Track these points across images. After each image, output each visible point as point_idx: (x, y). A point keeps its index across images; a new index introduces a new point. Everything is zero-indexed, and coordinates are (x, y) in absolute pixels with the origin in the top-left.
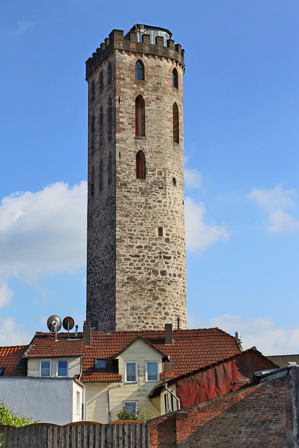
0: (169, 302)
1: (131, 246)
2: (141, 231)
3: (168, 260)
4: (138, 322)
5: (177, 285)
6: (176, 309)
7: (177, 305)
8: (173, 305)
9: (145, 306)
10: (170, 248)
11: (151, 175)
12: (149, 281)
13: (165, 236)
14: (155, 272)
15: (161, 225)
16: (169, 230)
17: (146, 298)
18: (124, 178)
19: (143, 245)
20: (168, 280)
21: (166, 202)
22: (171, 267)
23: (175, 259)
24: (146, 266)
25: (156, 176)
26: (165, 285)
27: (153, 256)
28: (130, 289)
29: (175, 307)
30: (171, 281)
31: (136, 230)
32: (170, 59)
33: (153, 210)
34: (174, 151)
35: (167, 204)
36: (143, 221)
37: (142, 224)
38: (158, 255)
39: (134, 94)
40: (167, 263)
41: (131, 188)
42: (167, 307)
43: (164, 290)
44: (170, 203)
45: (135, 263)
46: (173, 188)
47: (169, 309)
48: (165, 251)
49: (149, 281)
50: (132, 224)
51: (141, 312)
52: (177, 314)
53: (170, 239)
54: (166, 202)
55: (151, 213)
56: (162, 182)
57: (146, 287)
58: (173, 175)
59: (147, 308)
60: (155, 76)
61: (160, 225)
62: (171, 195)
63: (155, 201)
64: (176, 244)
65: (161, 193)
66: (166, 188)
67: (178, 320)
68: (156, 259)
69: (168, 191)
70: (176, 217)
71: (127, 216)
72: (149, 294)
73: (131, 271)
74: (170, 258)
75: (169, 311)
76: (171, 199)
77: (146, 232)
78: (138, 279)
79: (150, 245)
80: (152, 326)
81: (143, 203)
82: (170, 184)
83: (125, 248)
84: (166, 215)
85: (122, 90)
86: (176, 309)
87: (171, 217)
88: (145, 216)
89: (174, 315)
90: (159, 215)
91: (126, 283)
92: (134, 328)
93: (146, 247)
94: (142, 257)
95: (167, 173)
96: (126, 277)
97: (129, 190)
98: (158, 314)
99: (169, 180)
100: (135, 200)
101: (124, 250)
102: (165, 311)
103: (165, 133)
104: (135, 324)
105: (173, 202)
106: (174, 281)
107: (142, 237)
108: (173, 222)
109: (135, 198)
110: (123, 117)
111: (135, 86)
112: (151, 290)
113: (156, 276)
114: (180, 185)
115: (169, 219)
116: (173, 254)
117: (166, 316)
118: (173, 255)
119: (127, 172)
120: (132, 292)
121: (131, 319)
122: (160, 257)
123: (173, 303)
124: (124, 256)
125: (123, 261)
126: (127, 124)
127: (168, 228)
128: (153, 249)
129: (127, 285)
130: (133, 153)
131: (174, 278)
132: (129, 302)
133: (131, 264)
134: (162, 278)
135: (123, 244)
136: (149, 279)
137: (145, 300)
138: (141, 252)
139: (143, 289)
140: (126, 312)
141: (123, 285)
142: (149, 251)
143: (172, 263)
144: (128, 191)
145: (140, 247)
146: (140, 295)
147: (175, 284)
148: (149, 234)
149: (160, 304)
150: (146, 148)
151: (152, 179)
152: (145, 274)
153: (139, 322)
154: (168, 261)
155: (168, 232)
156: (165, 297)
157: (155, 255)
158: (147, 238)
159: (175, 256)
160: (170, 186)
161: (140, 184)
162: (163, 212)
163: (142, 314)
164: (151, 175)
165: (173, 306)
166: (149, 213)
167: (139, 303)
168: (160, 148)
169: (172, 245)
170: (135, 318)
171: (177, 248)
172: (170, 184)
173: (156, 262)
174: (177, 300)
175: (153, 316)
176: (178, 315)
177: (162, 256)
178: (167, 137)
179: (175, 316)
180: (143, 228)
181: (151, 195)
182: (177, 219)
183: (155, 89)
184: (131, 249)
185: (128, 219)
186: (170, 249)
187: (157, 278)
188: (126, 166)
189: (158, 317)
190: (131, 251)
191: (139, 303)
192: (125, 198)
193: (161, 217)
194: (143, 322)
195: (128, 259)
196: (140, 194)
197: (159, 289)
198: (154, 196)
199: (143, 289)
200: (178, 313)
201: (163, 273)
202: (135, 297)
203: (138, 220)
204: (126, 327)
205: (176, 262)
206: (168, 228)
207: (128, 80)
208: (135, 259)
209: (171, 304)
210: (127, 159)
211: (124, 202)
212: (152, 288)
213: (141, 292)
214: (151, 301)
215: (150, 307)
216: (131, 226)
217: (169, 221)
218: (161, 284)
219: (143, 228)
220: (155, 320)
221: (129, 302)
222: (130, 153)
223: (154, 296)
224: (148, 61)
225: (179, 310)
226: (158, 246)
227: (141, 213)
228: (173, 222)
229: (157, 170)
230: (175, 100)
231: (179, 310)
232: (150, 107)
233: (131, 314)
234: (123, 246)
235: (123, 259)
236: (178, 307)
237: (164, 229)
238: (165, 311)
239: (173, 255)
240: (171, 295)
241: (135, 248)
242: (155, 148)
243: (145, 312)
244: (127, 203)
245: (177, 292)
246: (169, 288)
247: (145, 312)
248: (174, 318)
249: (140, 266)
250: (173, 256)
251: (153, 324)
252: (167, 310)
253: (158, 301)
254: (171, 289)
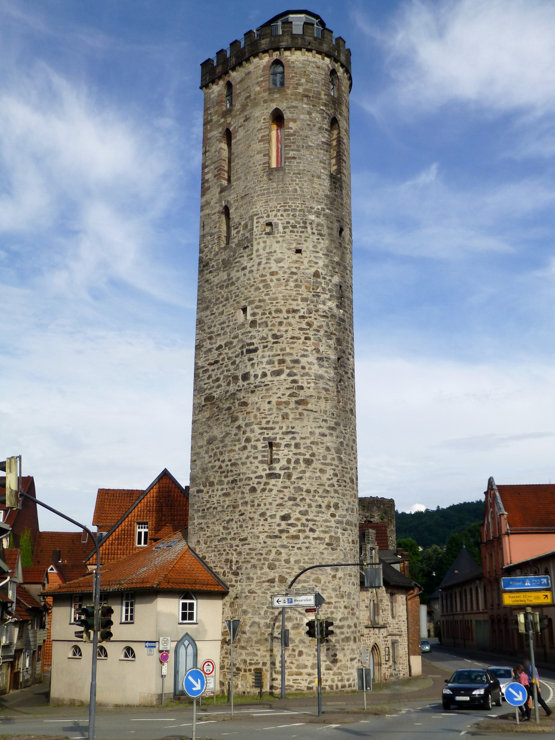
0: (252, 420)
1: (210, 350)
2: (220, 324)
3: (253, 354)
4: (213, 461)
5: (267, 390)
6: (266, 428)
7: (268, 422)
8: (260, 423)
9: (222, 435)
10: (256, 334)
11: (235, 235)
12: (228, 394)
14: (236, 378)
15: (244, 304)
16: (257, 307)
17: (223, 423)
18: (207, 256)
19: (223, 343)
20: (252, 386)
21: (253, 266)
22: (258, 364)
23: (266, 349)
24: (225, 373)
25: (242, 232)
26: (247, 395)
27: (234, 355)
28: (207, 414)
29: (264, 425)
30: (256, 387)
31: (217, 323)
32: (283, 49)
33: (236, 285)
34: (270, 182)
35: (254, 268)
36: (224, 308)
37: (222, 313)
38: (240, 351)
39: (220, 133)
40: (250, 359)
42: (248, 429)
43: (245, 404)
44: (259, 264)
45: (214, 373)
46: (264, 240)
47: (252, 431)
48: (249, 341)
49: (228, 394)
50: (212, 317)
51: (217, 446)
52: (267, 436)
53: (258, 321)
54: (253, 266)
55: (234, 291)
56: (247, 237)
57: (224, 406)
58: (267, 219)
59: (224, 437)
60: (243, 91)
61: (243, 303)
62: (261, 252)
63: (238, 271)
64: (270, 324)
65: (245, 255)
66: (252, 245)
67: (271, 445)
68: (237, 359)
69: (255, 248)
70: (272, 281)
72: (227, 416)
73: (209, 387)
74: (256, 350)
75: (252, 435)
76: (261, 257)
77: (227, 322)
78: (216, 396)
79: (231, 340)
80: (229, 463)
81: (225, 281)
82: (260, 234)
83: (204, 356)
84: (253, 285)
86: (266, 428)
87: (261, 285)
88: (227, 299)
89: (261, 439)
90: (243, 289)
91: (204, 406)
92: (209, 471)
93: (226, 345)
94: (221, 362)
95: (255, 221)
96: (203, 398)
97: (211, 269)
98: (237, 443)
100: (216, 280)
101: (202, 360)
102: (245, 436)
103: (254, 163)
104: (210, 465)
105: (264, 261)
106: (262, 385)
107: (223, 332)
108: (263, 292)
109: (216, 279)
111: (222, 120)
112: (229, 408)
113: (236, 384)
114: (284, 228)
115: (258, 289)
116: (263, 341)
117: (247, 444)
118: (262, 343)
119: (210, 246)
120: (209, 419)
121: (207, 459)
122: (242, 352)
123: (259, 420)
124: (203, 367)
125: (201, 375)
126: (213, 178)
127: (255, 304)
128: (234, 345)
129: (204, 408)
130: (217, 214)
131: (263, 380)
132: (205, 434)
133: (209, 377)
134: (243, 386)
135: (202, 351)
136: (228, 391)
137: (223, 425)
138: (220, 354)
139: (220, 409)
140: (201, 450)
141: (200, 411)
142: (229, 349)
143: (260, 356)
144: (210, 272)
145: (220, 347)
146: (217, 420)
147: (265, 388)
148: (231, 323)
149: (239, 427)
151: (236, 240)
153: (215, 461)
154: (252, 355)
155: (256, 310)
156: (247, 413)
157: (237, 353)
158: (228, 330)
159: (265, 344)
160: (259, 238)
162: (249, 282)
163: (218, 448)
164: (235, 235)
165: (259, 426)
166: (231, 291)
167: (217, 432)
168: (246, 189)
169: (261, 329)
170: (210, 457)
171: (271, 330)
172: (260, 234)
173: (237, 363)
174: (267, 413)
175: (230, 448)
176: (269, 438)
177: (245, 352)
178: (258, 167)
179: (262, 441)
180: (224, 318)
181: (234, 265)
182: (272, 284)
184: (209, 354)
185: (208, 312)
186: (257, 336)
187: (237, 388)
188: (209, 238)
189: (237, 448)
190: (210, 357)
191: (217, 432)
192: (206, 284)
193: (246, 291)
194: (219, 460)
195: (207, 370)
196: (222, 269)
197: (239, 405)
198: (237, 264)
200: (270, 435)
201: (246, 377)
202: (211, 424)
203: (218, 309)
204: (200, 471)
205: (267, 353)
206: (255, 304)
207: (215, 118)
209: (256, 423)
210: (210, 227)
211: (205, 289)
212: (231, 405)
213: (218, 415)
214: (228, 426)
215: (228, 434)
216: (211, 321)
217: (257, 293)
218: (241, 395)
219: (224, 318)
220: (232, 454)
221: (205, 434)
222: (213, 217)
223: (232, 417)
225: (272, 429)
226: (240, 337)
227: (223, 297)
228: (263, 292)
229: (243, 223)
230: (274, 106)
231: (272, 429)
232: (238, 138)
233: (207, 452)
234: (201, 353)
235: (201, 373)
236: (271, 425)
237: (249, 309)
238: (245, 436)
239: (262, 343)
240: (255, 409)
241: (214, 351)
242: (241, 192)
243: (222, 444)
244: (208, 291)
245: (267, 400)
246: (252, 399)
247: (221, 445)
248: (260, 445)
249: (219, 376)
250: (262, 345)
251: (230, 460)
252: (248, 434)
253: (237, 424)
254: (257, 399)
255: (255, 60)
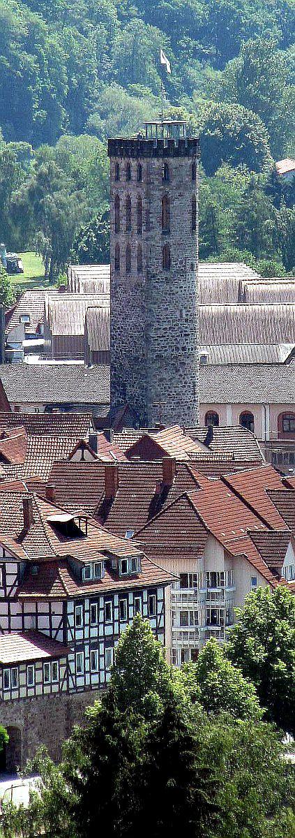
13: (184, 316)
14: (177, 349)
28: (158, 365)
35: (187, 289)
41: (158, 279)
71: (155, 303)
85: (152, 192)
99: (188, 267)
110: (152, 217)
145: (165, 329)
149: (181, 375)
150: (171, 241)
152: (169, 351)
161: (167, 275)
183: (178, 187)
185: (156, 306)
199: (168, 365)
201: (184, 349)
207: (156, 183)
208: (162, 339)
224: (172, 161)
255: (186, 158)
